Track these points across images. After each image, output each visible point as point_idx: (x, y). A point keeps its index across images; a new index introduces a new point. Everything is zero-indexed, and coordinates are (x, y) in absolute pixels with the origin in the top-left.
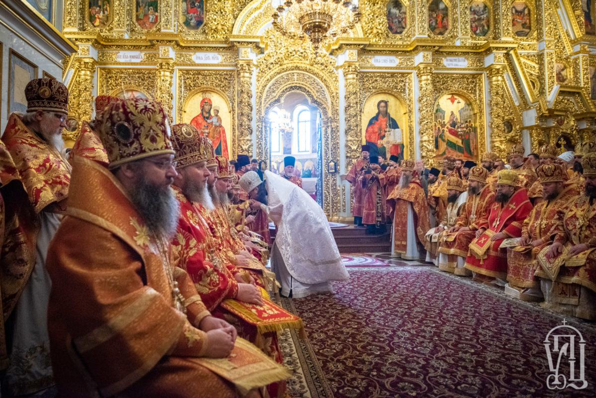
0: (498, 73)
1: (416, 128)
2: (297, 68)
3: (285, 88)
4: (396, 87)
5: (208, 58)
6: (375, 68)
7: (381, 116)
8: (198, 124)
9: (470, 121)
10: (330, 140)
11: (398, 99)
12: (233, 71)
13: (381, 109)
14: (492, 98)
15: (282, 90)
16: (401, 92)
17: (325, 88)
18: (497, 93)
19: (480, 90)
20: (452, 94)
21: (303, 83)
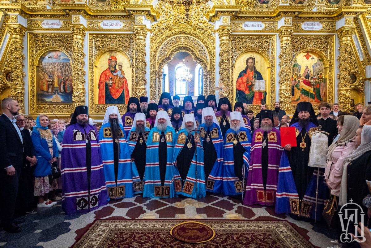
0: (348, 34)
1: (277, 79)
2: (183, 32)
3: (174, 48)
4: (262, 47)
5: (112, 25)
6: (245, 31)
7: (249, 70)
9: (321, 74)
10: (208, 88)
11: (262, 56)
12: (132, 34)
13: (249, 64)
14: (341, 55)
15: (172, 50)
16: (266, 50)
17: (205, 48)
18: (346, 51)
19: (331, 49)
20: (308, 52)
21: (188, 44)
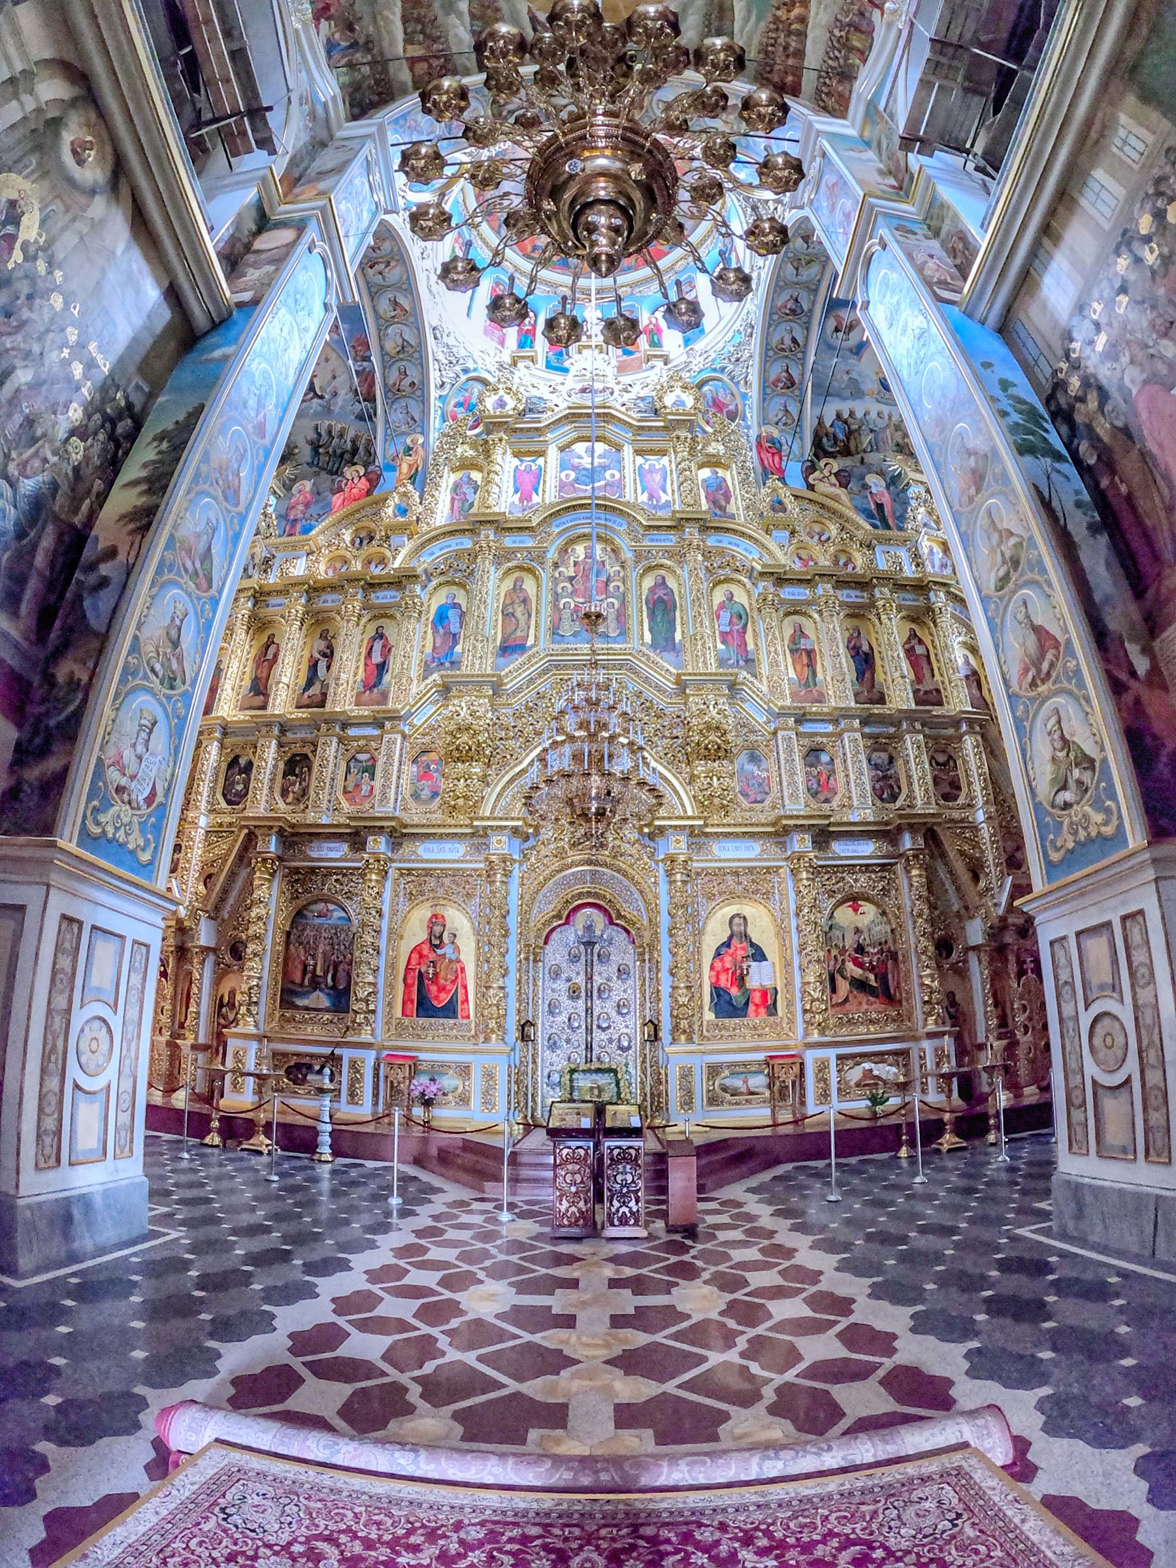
7: (735, 941)
8: (421, 956)
13: (735, 928)
